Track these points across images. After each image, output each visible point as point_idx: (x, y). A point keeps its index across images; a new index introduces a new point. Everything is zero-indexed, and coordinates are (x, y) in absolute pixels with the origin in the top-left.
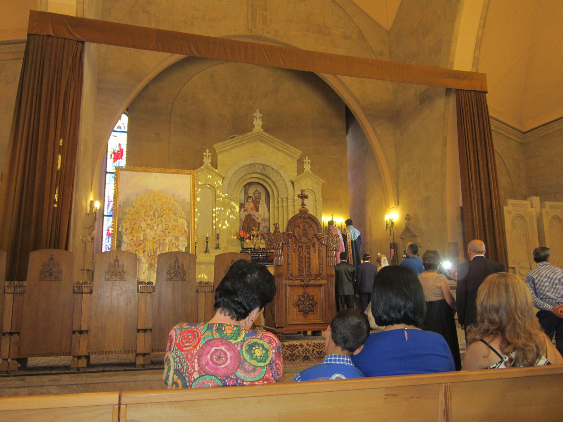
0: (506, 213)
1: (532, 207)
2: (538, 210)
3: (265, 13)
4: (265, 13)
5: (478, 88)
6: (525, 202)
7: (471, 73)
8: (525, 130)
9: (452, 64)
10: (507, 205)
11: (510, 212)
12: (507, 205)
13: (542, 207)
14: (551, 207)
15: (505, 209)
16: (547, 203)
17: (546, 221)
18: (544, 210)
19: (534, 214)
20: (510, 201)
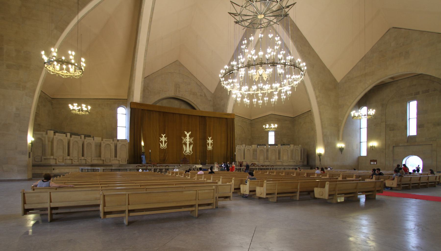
0: (236, 148)
1: (243, 147)
2: (244, 148)
3: (179, 89)
4: (179, 89)
5: (232, 118)
6: (241, 146)
7: (232, 114)
8: (252, 119)
9: (227, 111)
10: (236, 146)
11: (237, 148)
12: (236, 146)
13: (245, 147)
14: (248, 147)
15: (236, 147)
16: (247, 146)
17: (246, 150)
18: (246, 148)
19: (243, 149)
20: (238, 146)
